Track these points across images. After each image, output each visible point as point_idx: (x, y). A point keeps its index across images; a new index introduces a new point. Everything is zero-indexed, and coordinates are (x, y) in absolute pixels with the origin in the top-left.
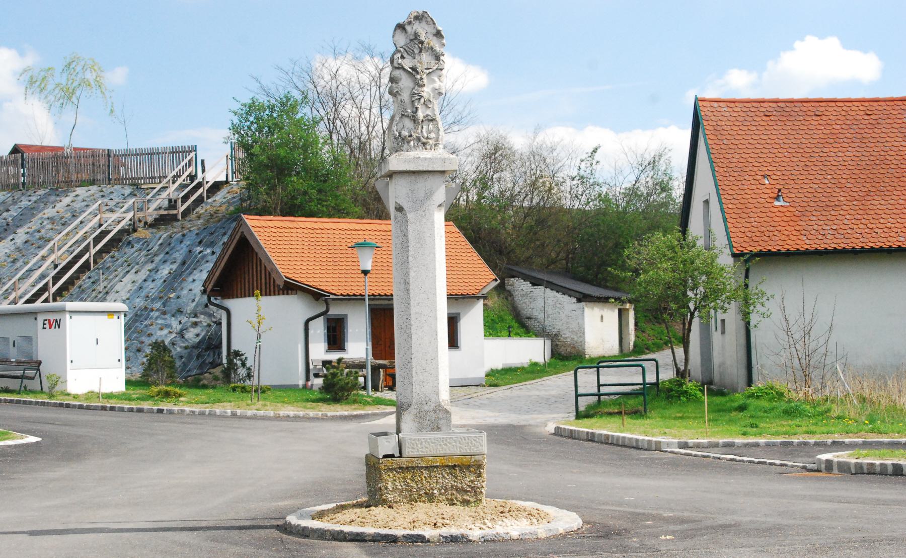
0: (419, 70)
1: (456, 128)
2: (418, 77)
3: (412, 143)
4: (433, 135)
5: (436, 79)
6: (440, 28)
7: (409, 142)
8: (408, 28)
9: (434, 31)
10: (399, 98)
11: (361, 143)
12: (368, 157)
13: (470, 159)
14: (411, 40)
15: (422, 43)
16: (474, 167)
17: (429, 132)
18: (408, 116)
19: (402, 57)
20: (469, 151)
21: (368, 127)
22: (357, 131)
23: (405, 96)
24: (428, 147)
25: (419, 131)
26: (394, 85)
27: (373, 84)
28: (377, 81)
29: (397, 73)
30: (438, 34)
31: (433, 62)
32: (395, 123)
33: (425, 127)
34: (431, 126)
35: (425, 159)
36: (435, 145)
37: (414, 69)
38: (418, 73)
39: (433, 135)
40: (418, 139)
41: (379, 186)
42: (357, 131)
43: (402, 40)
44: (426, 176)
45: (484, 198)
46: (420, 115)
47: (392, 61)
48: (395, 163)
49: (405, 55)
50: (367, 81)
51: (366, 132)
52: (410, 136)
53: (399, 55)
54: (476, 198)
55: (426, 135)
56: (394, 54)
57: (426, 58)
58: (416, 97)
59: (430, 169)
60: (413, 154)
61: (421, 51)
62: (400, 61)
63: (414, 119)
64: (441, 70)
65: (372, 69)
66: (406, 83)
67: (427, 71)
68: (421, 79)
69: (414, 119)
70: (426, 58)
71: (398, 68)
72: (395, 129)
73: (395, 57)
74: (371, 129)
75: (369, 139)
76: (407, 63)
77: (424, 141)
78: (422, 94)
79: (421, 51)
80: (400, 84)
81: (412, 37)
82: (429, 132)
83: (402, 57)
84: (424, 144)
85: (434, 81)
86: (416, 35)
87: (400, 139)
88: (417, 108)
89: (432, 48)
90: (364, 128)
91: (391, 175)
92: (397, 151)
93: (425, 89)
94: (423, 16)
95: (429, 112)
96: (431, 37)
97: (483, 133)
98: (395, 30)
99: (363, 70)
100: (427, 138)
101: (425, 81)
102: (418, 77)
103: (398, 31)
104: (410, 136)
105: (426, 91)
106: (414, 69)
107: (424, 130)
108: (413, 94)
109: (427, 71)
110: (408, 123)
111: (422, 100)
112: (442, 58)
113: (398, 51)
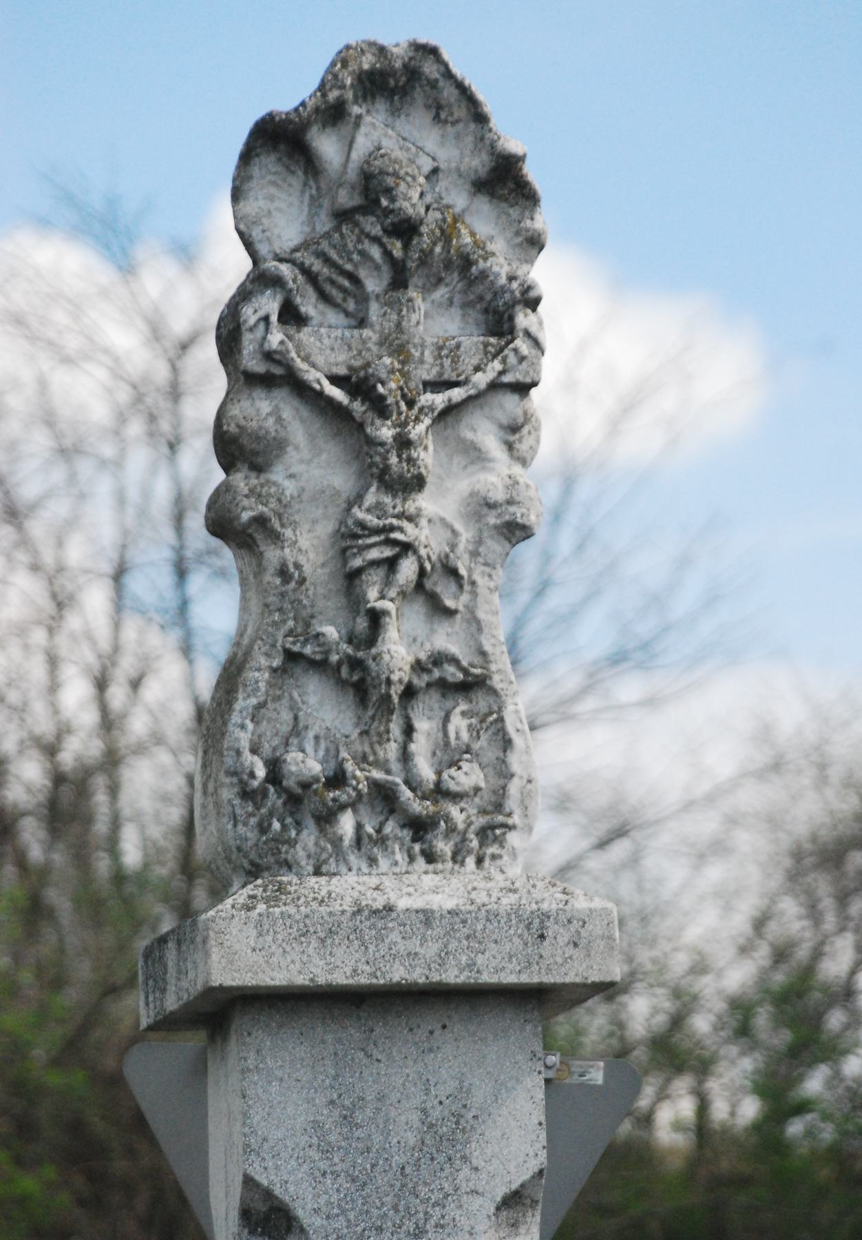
0: (389, 389)
1: (629, 688)
2: (386, 432)
3: (346, 824)
4: (468, 776)
5: (489, 439)
6: (513, 144)
7: (326, 818)
8: (327, 146)
9: (479, 163)
10: (272, 555)
11: (59, 779)
12: (102, 865)
13: (715, 873)
14: (343, 216)
15: (406, 229)
16: (740, 922)
17: (450, 756)
18: (320, 665)
19: (291, 316)
20: (707, 825)
21: (101, 684)
22: (39, 708)
23: (307, 544)
24: (444, 847)
25: (391, 750)
26: (241, 481)
27: (136, 428)
28: (153, 406)
29: (262, 409)
30: (505, 181)
31: (472, 342)
32: (244, 703)
33: (424, 726)
34: (458, 724)
35: (427, 917)
36: (485, 834)
37: (358, 384)
38: (380, 408)
39: (468, 776)
40: (384, 796)
41: (150, 1076)
42: (39, 708)
43: (288, 222)
44: (428, 1021)
45: (802, 1108)
46: (398, 650)
47: (229, 337)
48: (244, 945)
49: (308, 305)
50: (99, 412)
51: (88, 718)
52: (338, 779)
53: (270, 304)
54: (750, 1109)
55: (425, 770)
56: (243, 295)
57: (434, 321)
58: (366, 552)
59: (452, 976)
60: (351, 885)
61: (399, 281)
62: (276, 338)
63: (359, 682)
64: (523, 389)
65: (126, 340)
66: (311, 470)
67: (439, 400)
68: (404, 443)
69: (359, 682)
70: (434, 321)
71: (264, 381)
72: (244, 739)
73: (250, 315)
74: (117, 695)
75: (112, 761)
76: (322, 349)
77: (418, 807)
78: (410, 532)
79: (399, 281)
80: (277, 475)
81: (346, 199)
82: (450, 756)
83: (291, 316)
84: (419, 827)
85: (475, 455)
86: (373, 187)
87: (274, 798)
88: (376, 619)
89: (466, 262)
90: (76, 694)
91: (222, 1014)
92: (254, 872)
93: (424, 502)
94: (412, 73)
95: (448, 639)
96: (458, 199)
97: (791, 718)
98: (246, 157)
99: (72, 343)
100: (440, 792)
101: (428, 457)
102: (386, 432)
103: (267, 164)
104: (338, 779)
105: (437, 515)
106: (358, 384)
107: (421, 747)
108: (349, 537)
109: (439, 400)
110: (325, 709)
111: (407, 570)
112: (523, 319)
113: (260, 280)
